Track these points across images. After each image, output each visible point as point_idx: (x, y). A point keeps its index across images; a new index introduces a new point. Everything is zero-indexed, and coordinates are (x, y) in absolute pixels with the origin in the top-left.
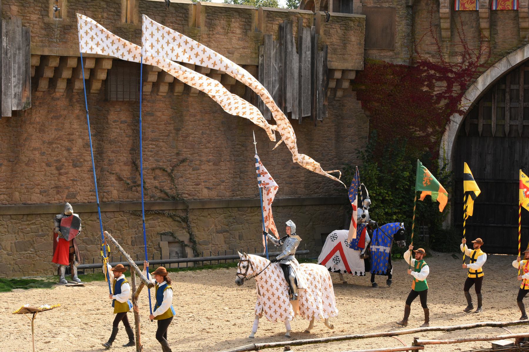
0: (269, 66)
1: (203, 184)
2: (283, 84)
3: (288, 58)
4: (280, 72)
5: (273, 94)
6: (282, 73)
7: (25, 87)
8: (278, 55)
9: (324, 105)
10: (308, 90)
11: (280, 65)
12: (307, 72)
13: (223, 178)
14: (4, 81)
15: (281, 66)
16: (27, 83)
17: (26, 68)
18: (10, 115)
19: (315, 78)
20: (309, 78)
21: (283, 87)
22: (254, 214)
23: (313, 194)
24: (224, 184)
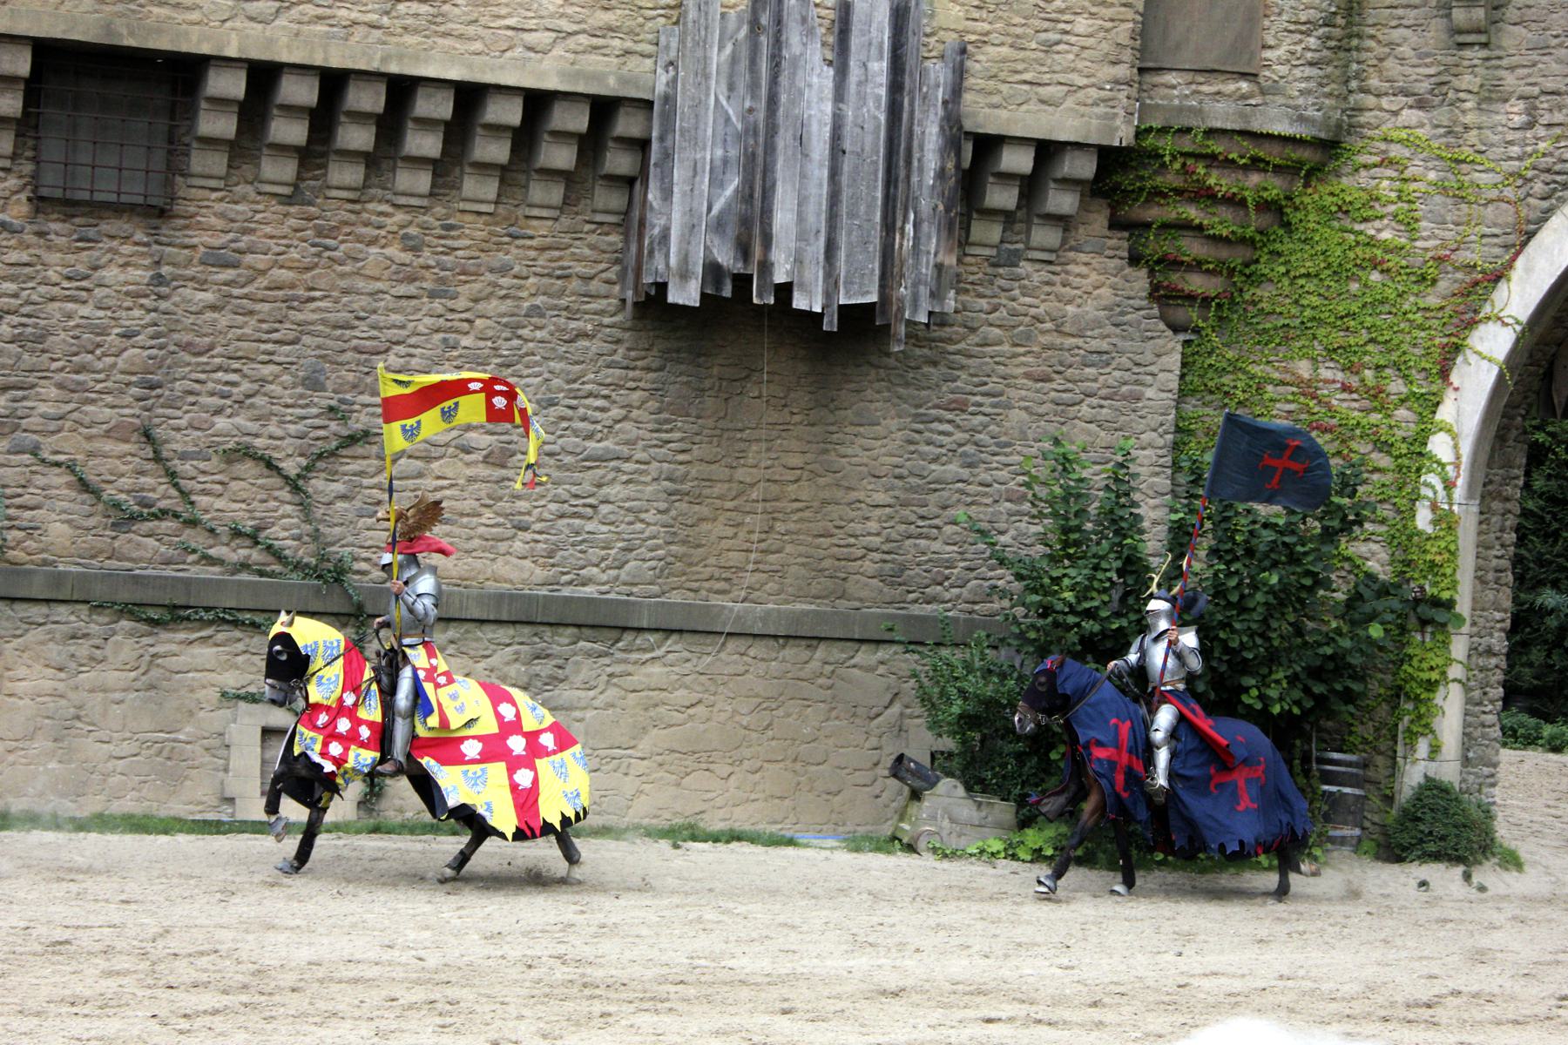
0: (698, 105)
2: (758, 177)
3: (784, 80)
4: (746, 131)
5: (715, 211)
6: (756, 133)
8: (744, 64)
9: (939, 267)
10: (870, 206)
11: (747, 104)
12: (869, 139)
13: (520, 513)
15: (751, 110)
19: (902, 163)
20: (876, 163)
22: (648, 656)
23: (916, 601)
24: (528, 536)
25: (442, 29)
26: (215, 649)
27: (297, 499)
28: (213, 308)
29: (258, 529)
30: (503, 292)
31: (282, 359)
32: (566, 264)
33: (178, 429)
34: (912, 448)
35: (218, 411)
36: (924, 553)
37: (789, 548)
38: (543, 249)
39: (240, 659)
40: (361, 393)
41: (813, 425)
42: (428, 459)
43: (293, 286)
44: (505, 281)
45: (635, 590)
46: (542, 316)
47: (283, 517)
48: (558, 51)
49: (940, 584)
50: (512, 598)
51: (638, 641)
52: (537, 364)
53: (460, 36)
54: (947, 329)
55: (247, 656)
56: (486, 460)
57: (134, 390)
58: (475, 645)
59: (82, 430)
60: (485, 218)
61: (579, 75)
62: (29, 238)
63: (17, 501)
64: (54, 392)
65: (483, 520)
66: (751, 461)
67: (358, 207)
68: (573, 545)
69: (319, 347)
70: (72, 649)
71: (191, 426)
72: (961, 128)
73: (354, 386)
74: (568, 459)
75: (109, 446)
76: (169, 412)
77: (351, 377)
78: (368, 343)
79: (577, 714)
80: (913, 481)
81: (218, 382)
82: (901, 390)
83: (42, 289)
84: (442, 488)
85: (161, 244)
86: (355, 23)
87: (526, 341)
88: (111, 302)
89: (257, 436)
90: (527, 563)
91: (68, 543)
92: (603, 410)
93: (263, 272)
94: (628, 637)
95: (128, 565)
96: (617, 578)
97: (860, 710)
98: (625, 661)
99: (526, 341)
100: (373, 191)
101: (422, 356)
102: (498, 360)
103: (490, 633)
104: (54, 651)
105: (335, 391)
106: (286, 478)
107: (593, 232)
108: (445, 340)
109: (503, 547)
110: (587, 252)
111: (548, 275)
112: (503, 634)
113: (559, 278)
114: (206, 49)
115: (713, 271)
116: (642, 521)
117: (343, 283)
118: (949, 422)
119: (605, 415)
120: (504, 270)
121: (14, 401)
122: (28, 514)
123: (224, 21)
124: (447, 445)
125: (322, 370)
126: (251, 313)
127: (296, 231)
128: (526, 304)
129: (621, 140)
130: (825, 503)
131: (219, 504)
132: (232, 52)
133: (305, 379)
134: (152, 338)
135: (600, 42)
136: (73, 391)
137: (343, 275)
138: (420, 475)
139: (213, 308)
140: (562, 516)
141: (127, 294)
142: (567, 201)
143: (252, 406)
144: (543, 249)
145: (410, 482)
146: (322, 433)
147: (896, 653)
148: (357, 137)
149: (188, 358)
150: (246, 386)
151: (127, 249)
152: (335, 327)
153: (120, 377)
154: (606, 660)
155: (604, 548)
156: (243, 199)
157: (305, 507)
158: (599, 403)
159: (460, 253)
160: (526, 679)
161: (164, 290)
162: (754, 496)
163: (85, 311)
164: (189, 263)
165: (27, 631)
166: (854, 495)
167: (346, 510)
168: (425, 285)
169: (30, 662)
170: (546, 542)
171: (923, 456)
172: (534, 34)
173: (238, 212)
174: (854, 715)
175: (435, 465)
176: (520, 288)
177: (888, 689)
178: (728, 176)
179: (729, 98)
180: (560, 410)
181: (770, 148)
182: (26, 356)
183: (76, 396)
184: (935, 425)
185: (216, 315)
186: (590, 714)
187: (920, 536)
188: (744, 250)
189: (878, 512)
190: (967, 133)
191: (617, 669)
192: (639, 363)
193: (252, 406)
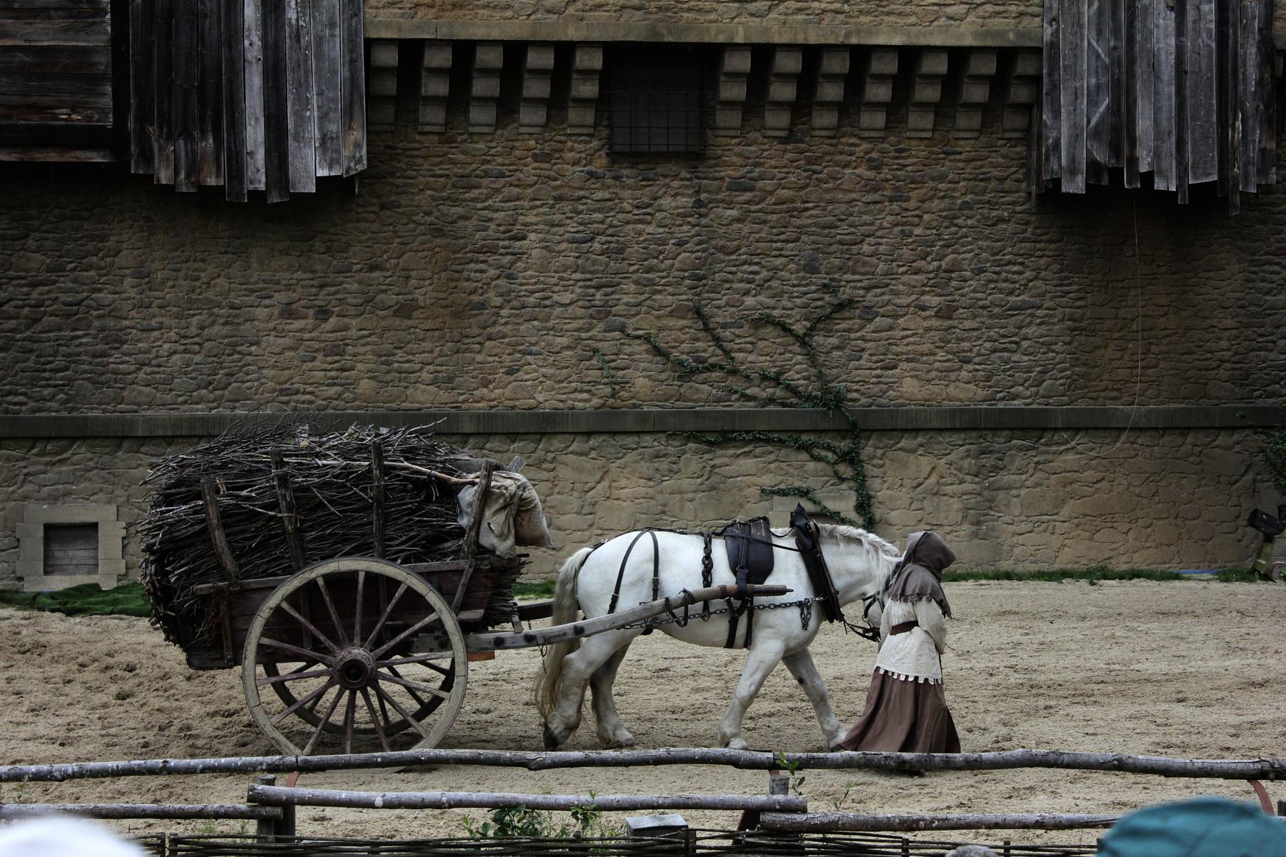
0: (1076, 47)
1: (904, 365)
2: (1123, 96)
3: (1138, 24)
4: (1112, 63)
7: (351, 119)
8: (1108, 15)
10: (1209, 111)
11: (1112, 44)
12: (1204, 62)
13: (964, 351)
14: (294, 105)
15: (1115, 48)
16: (356, 108)
17: (350, 71)
18: (312, 189)
20: (1211, 78)
21: (1123, 104)
22: (1063, 447)
23: (1260, 397)
24: (971, 367)
25: (886, 9)
26: (755, 460)
27: (805, 351)
28: (738, 220)
29: (779, 374)
30: (942, 194)
31: (788, 253)
32: (986, 170)
33: (719, 307)
34: (1250, 285)
35: (747, 293)
36: (1264, 362)
37: (1162, 364)
38: (968, 161)
39: (772, 466)
40: (845, 273)
41: (1174, 273)
42: (896, 317)
43: (792, 201)
44: (942, 186)
45: (1051, 401)
46: (971, 209)
47: (796, 364)
48: (971, 18)
49: (1278, 383)
50: (962, 412)
51: (1055, 438)
52: (969, 243)
53: (900, 14)
54: (1273, 196)
55: (776, 464)
56: (937, 315)
57: (687, 282)
58: (937, 447)
59: (653, 312)
60: (925, 142)
61: (987, 34)
62: (609, 181)
63: (613, 364)
64: (632, 287)
65: (938, 358)
66: (1130, 303)
67: (835, 141)
68: (1004, 371)
69: (813, 243)
70: (657, 465)
71: (728, 304)
72: (1274, 47)
73: (840, 269)
74: (996, 310)
75: (672, 322)
76: (712, 295)
77: (837, 262)
78: (848, 237)
79: (1014, 492)
80: (1253, 309)
81: (745, 272)
82: (1239, 243)
83: (620, 216)
84: (907, 336)
85: (699, 178)
86: (824, 11)
87: (961, 227)
88: (668, 222)
89: (774, 308)
90: (971, 386)
91: (649, 392)
92: (1020, 273)
93: (771, 193)
94: (1048, 435)
95: (691, 404)
96: (1037, 393)
97: (1222, 479)
98: (1047, 452)
99: (961, 227)
100: (845, 129)
101: (887, 244)
102: (942, 243)
103: (947, 438)
104: (645, 467)
105: (827, 273)
106: (797, 336)
107: (1005, 145)
108: (902, 231)
109: (953, 376)
110: (1001, 160)
111: (974, 179)
112: (956, 438)
113: (981, 180)
114: (721, 39)
115: (1093, 166)
116: (1053, 351)
117: (827, 197)
118: (1277, 264)
119: (1021, 277)
120: (942, 178)
121: (606, 295)
122: (621, 373)
123: (733, 18)
124: (908, 306)
125: (817, 258)
126: (764, 222)
127: (793, 161)
128: (959, 201)
129: (1020, 78)
130: (1187, 329)
131: (751, 358)
132: (739, 39)
133: (805, 266)
134: (697, 245)
135: (1001, 8)
136: (645, 286)
137: (827, 191)
138: (891, 328)
139: (738, 220)
140: (995, 351)
141: (678, 215)
142: (984, 127)
143: (769, 287)
144: (968, 161)
145: (884, 334)
146: (819, 303)
147: (1247, 436)
148: (831, 92)
149: (722, 257)
150: (764, 274)
151: (676, 184)
152: (824, 228)
153: (677, 273)
154: (1033, 453)
155: (1026, 372)
156: (755, 142)
157: (811, 357)
158: (1016, 268)
159: (909, 168)
160: (974, 469)
161: (703, 210)
162: (1134, 327)
163: (650, 229)
164: (719, 190)
165: (625, 454)
166: (1209, 322)
167: (840, 357)
168: (885, 193)
169: (629, 476)
170: (984, 370)
171: (1258, 290)
172: (953, 8)
173: (751, 152)
174: (1219, 482)
175: (901, 321)
176: (954, 190)
177: (1243, 462)
178: (1101, 97)
179: (1098, 41)
180: (989, 275)
181: (1131, 75)
182: (612, 264)
183: (647, 289)
184: (1266, 267)
185: (740, 225)
186: (1023, 492)
187: (1260, 349)
188: (1115, 150)
189: (1227, 333)
190: (1278, 51)
191: (1042, 458)
192: (1044, 238)
193: (769, 287)
